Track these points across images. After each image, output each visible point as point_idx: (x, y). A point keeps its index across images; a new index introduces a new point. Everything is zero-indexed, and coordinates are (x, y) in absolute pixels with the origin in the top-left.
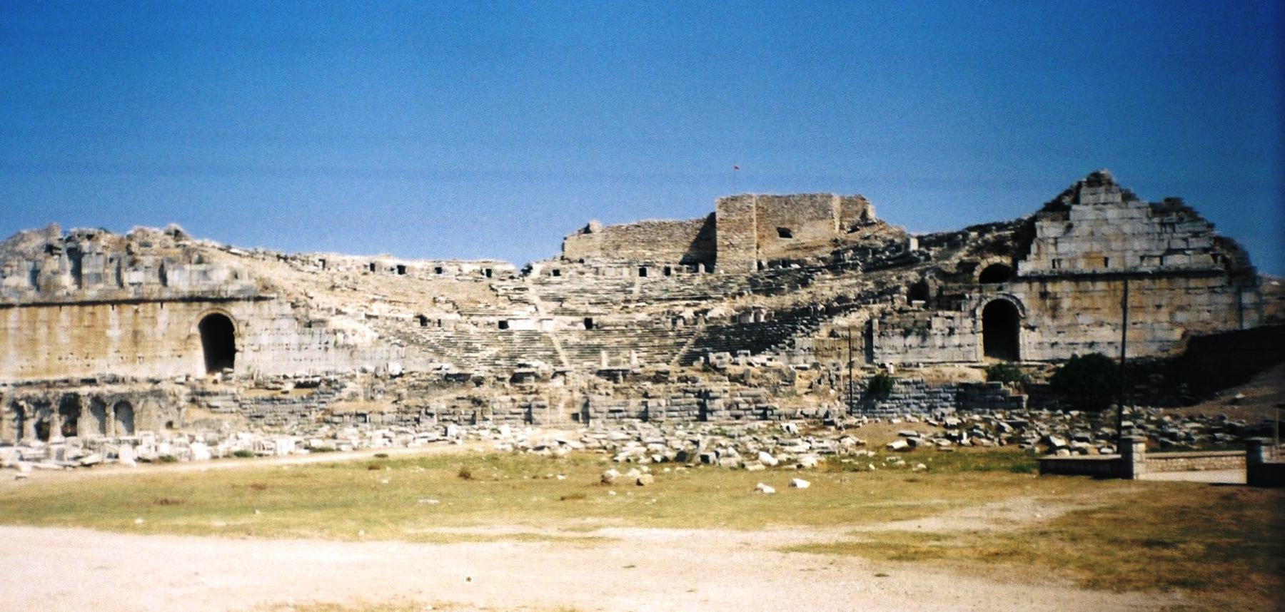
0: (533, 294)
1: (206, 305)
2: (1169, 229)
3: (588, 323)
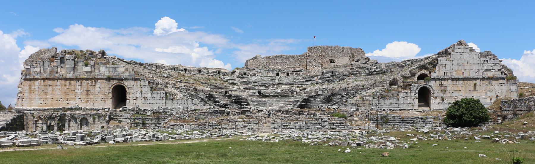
0: (237, 81)
1: (115, 81)
2: (486, 62)
3: (259, 92)
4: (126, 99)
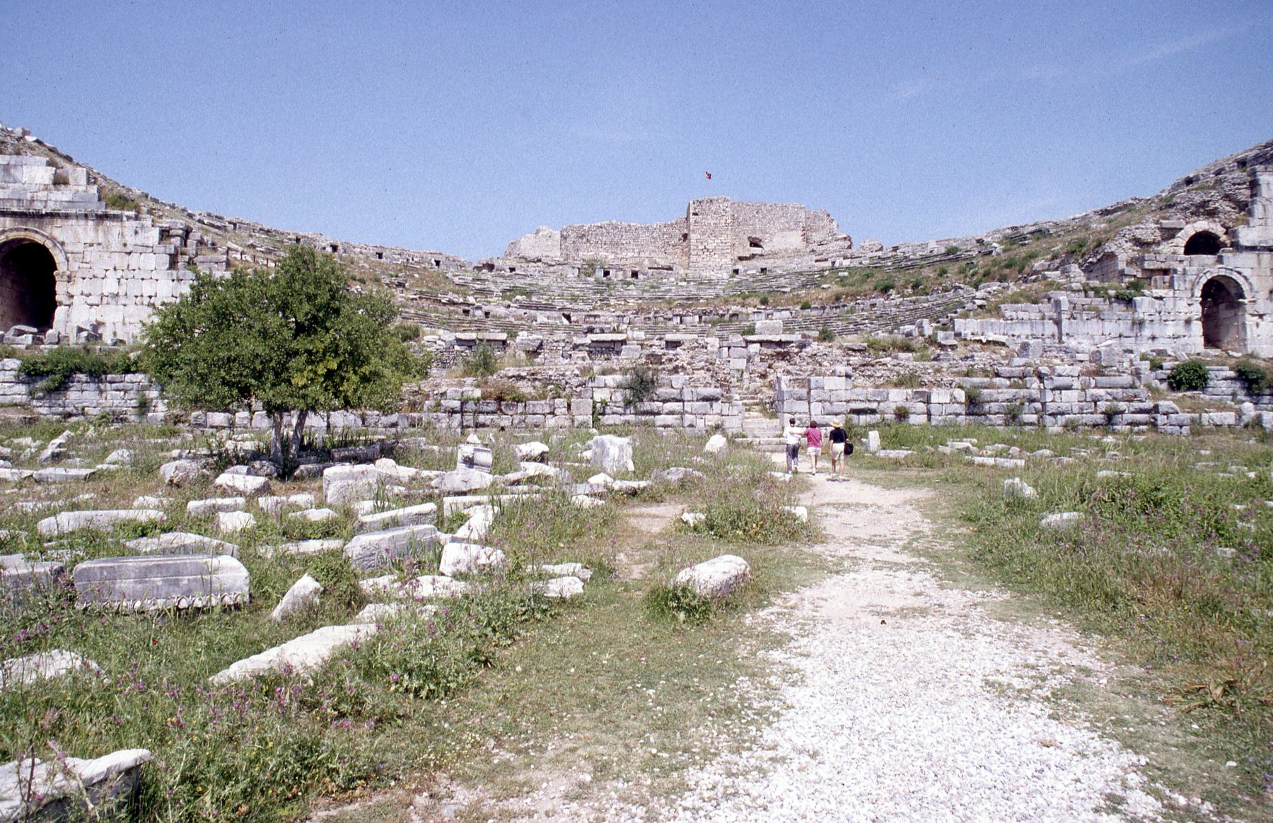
4: (54, 305)
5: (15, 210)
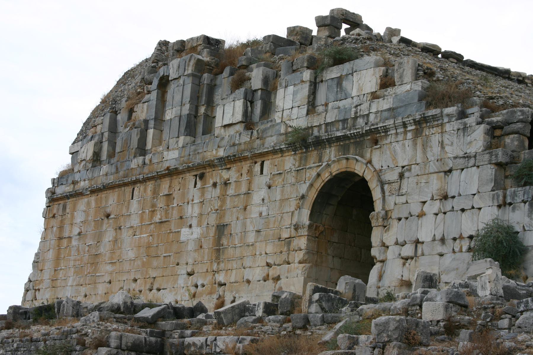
1: (331, 153)
5: (339, 134)
